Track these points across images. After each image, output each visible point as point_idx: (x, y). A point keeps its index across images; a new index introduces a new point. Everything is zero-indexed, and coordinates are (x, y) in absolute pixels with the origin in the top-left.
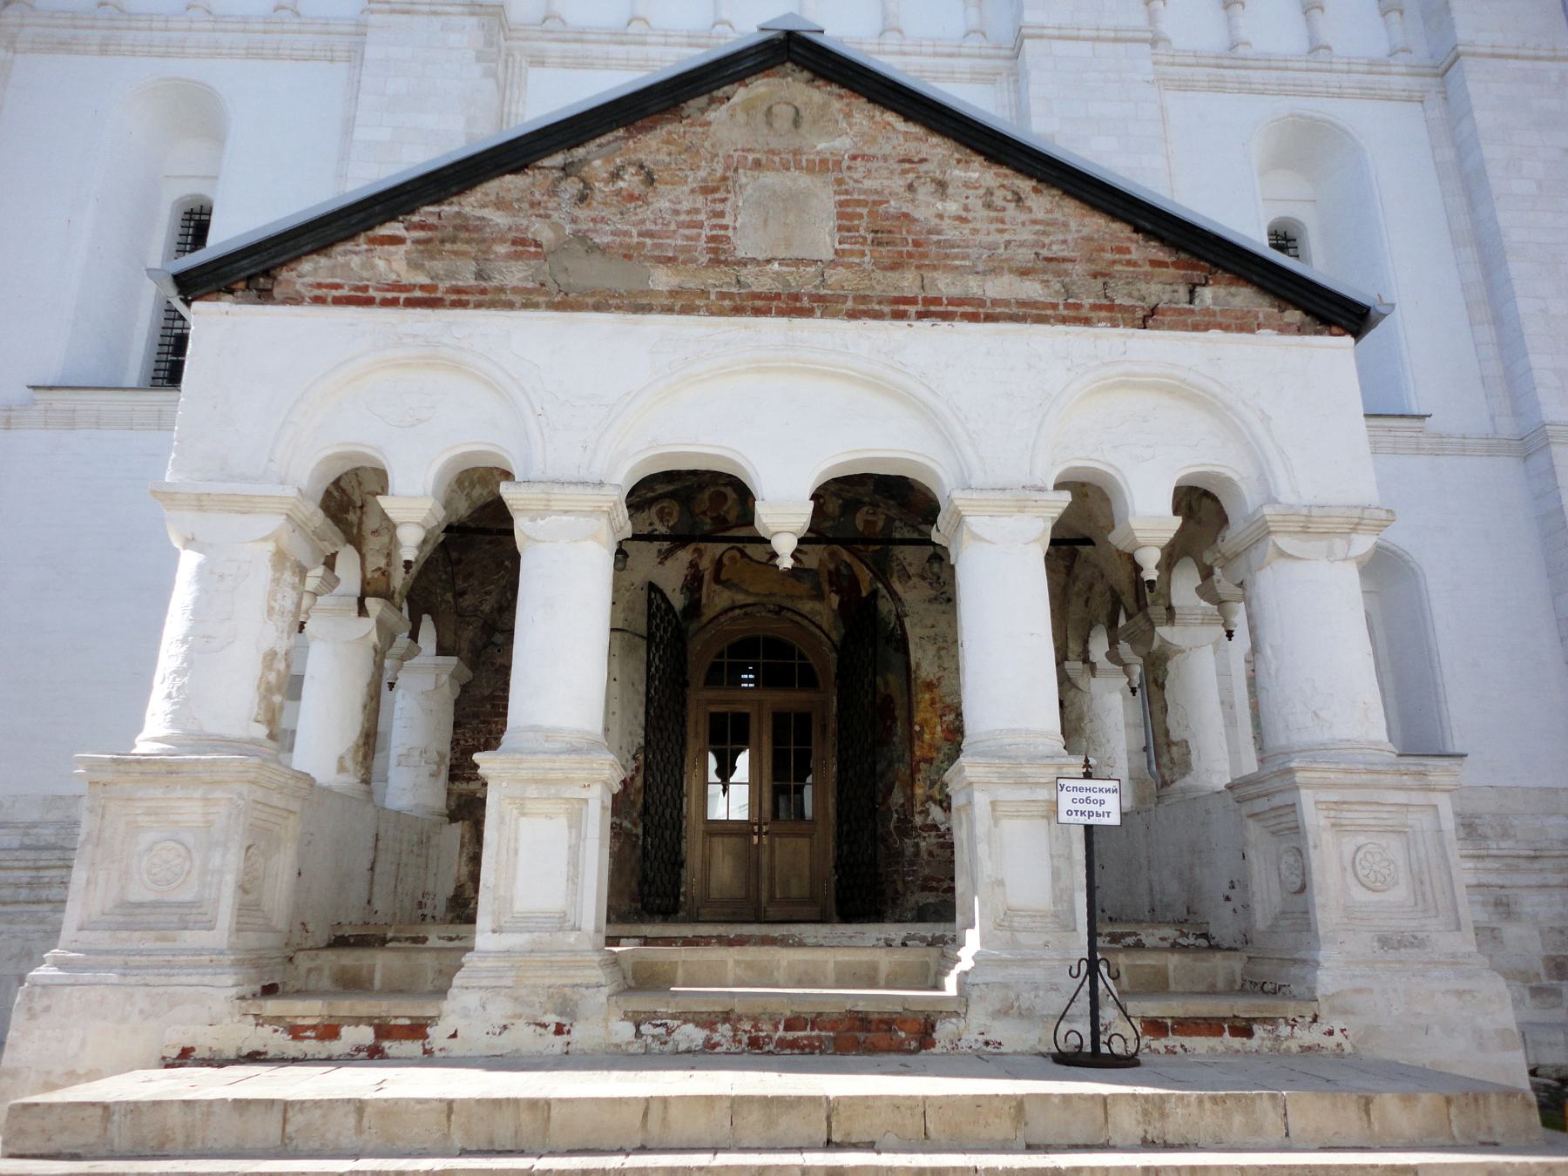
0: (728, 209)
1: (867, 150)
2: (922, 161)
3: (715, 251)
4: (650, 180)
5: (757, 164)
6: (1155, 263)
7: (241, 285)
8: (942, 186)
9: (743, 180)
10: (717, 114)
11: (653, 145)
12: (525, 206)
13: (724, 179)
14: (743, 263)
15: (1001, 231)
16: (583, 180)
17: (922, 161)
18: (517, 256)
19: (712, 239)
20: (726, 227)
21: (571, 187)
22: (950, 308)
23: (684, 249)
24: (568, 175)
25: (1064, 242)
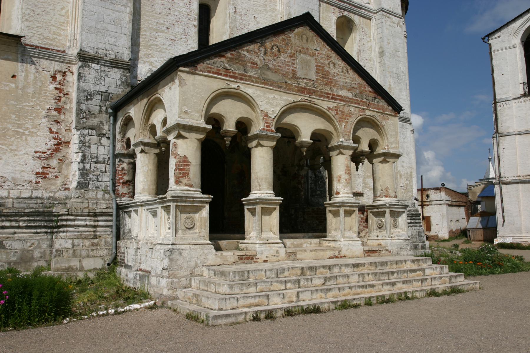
0: (295, 63)
1: (322, 52)
2: (331, 57)
3: (293, 74)
4: (279, 51)
5: (300, 52)
6: (370, 92)
7: (190, 64)
8: (334, 64)
9: (298, 55)
10: (292, 35)
11: (279, 40)
12: (253, 53)
13: (294, 54)
14: (299, 78)
15: (345, 79)
16: (265, 48)
17: (331, 57)
18: (253, 67)
19: (293, 70)
20: (295, 68)
21: (263, 49)
22: (337, 97)
23: (287, 72)
24: (262, 46)
25: (356, 84)
